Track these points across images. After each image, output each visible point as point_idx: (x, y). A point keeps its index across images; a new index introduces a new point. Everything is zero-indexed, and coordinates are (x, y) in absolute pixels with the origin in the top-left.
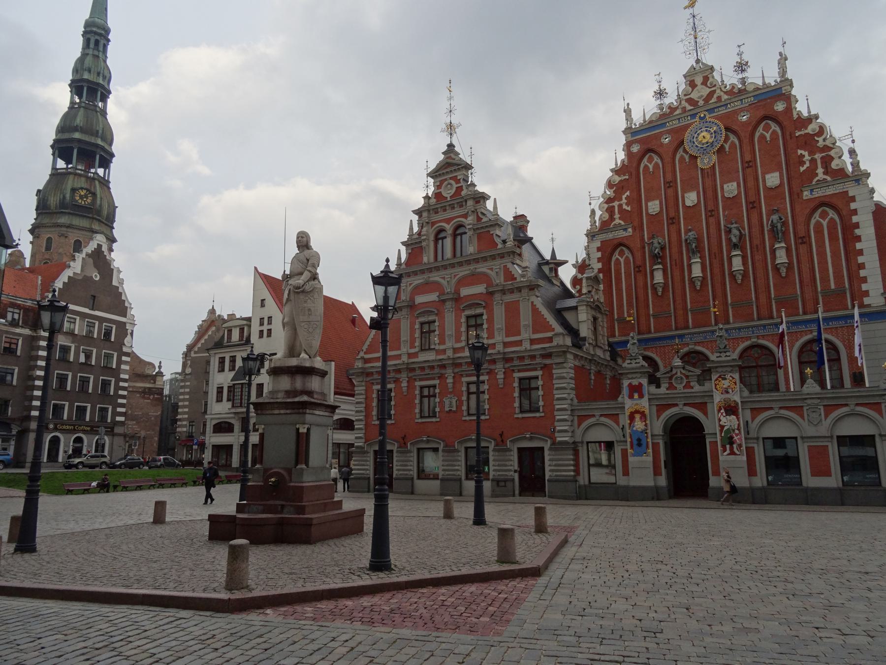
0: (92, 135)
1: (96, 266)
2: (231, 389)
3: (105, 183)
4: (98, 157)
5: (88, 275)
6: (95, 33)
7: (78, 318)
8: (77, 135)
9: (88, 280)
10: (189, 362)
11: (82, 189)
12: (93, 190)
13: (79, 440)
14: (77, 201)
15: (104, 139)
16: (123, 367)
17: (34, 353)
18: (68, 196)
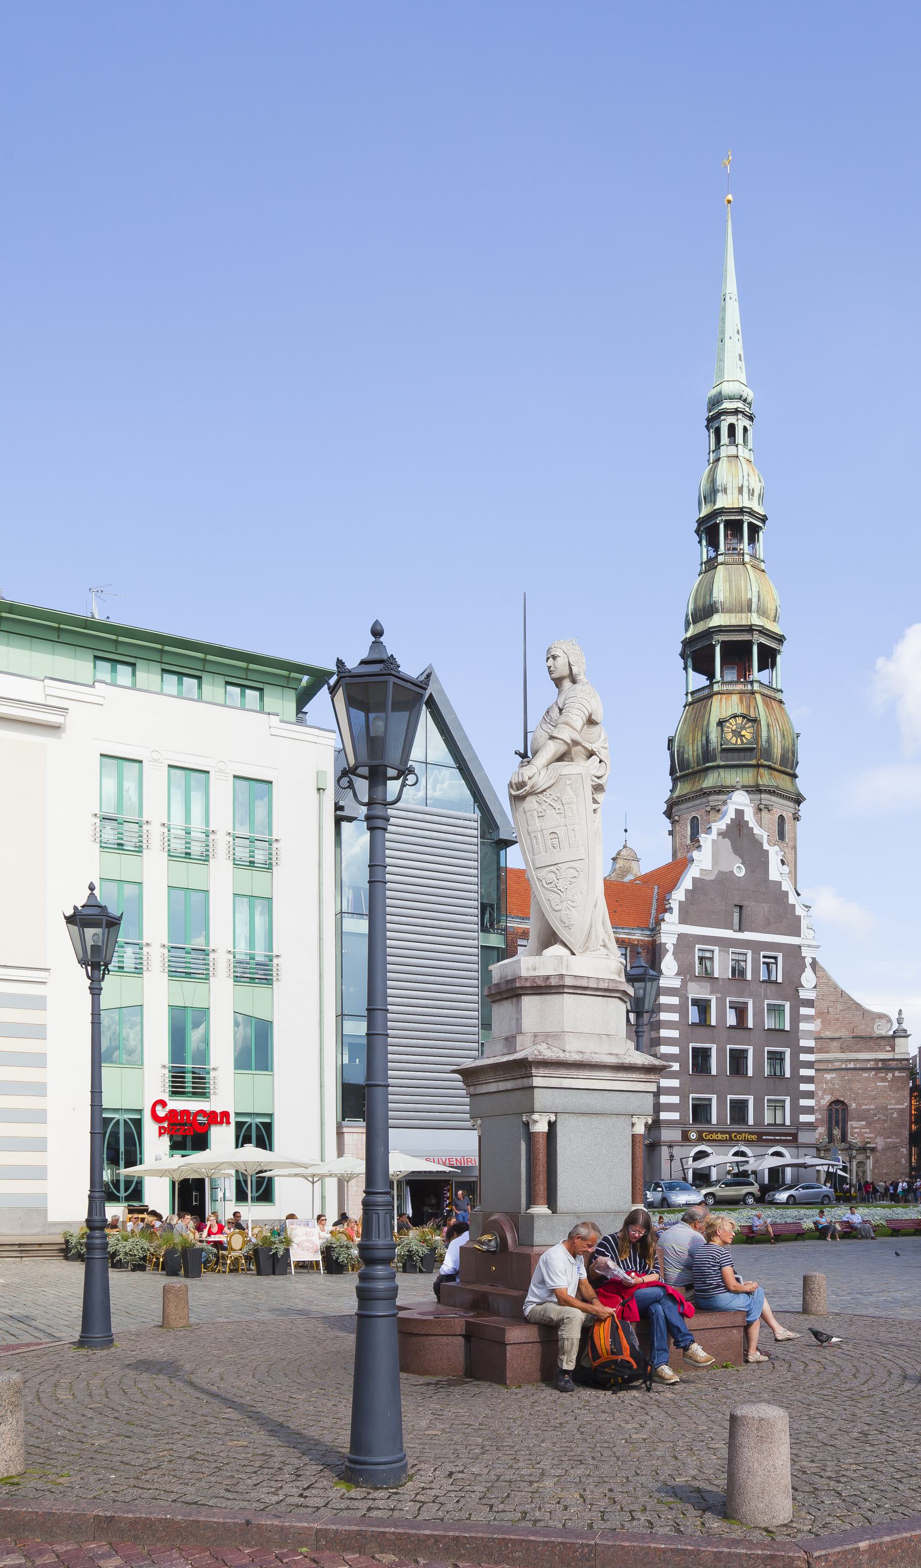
0: (741, 611)
3: (773, 697)
5: (726, 869)
8: (717, 620)
9: (725, 878)
12: (752, 714)
14: (729, 742)
15: (762, 612)
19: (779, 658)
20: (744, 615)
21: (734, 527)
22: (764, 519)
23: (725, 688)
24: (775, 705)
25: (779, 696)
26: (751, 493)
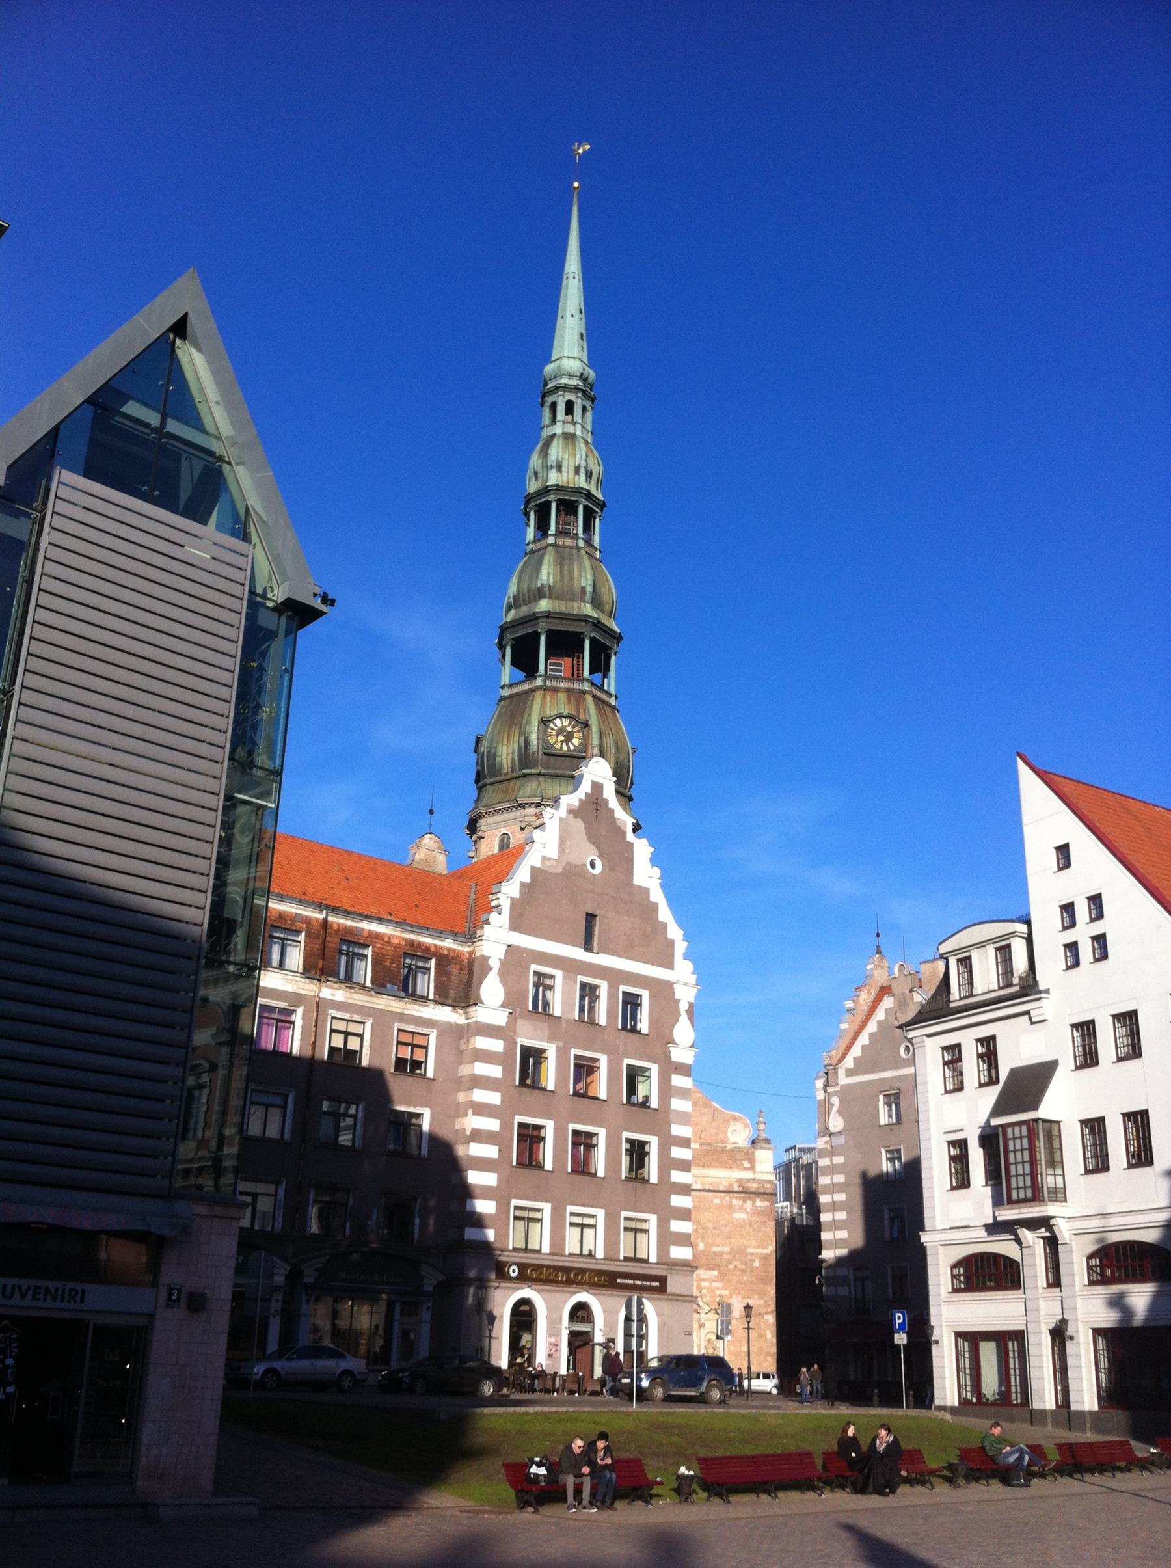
0: (572, 600)
1: (593, 838)
2: (990, 1139)
4: (587, 643)
5: (575, 859)
6: (565, 388)
7: (559, 974)
8: (544, 605)
9: (572, 874)
10: (835, 1101)
11: (561, 716)
13: (581, 1312)
15: (596, 602)
16: (677, 1104)
17: (465, 1070)
18: (534, 738)
19: (613, 659)
20: (575, 605)
21: (568, 508)
22: (602, 506)
23: (548, 683)
24: (608, 711)
25: (612, 701)
26: (589, 475)
